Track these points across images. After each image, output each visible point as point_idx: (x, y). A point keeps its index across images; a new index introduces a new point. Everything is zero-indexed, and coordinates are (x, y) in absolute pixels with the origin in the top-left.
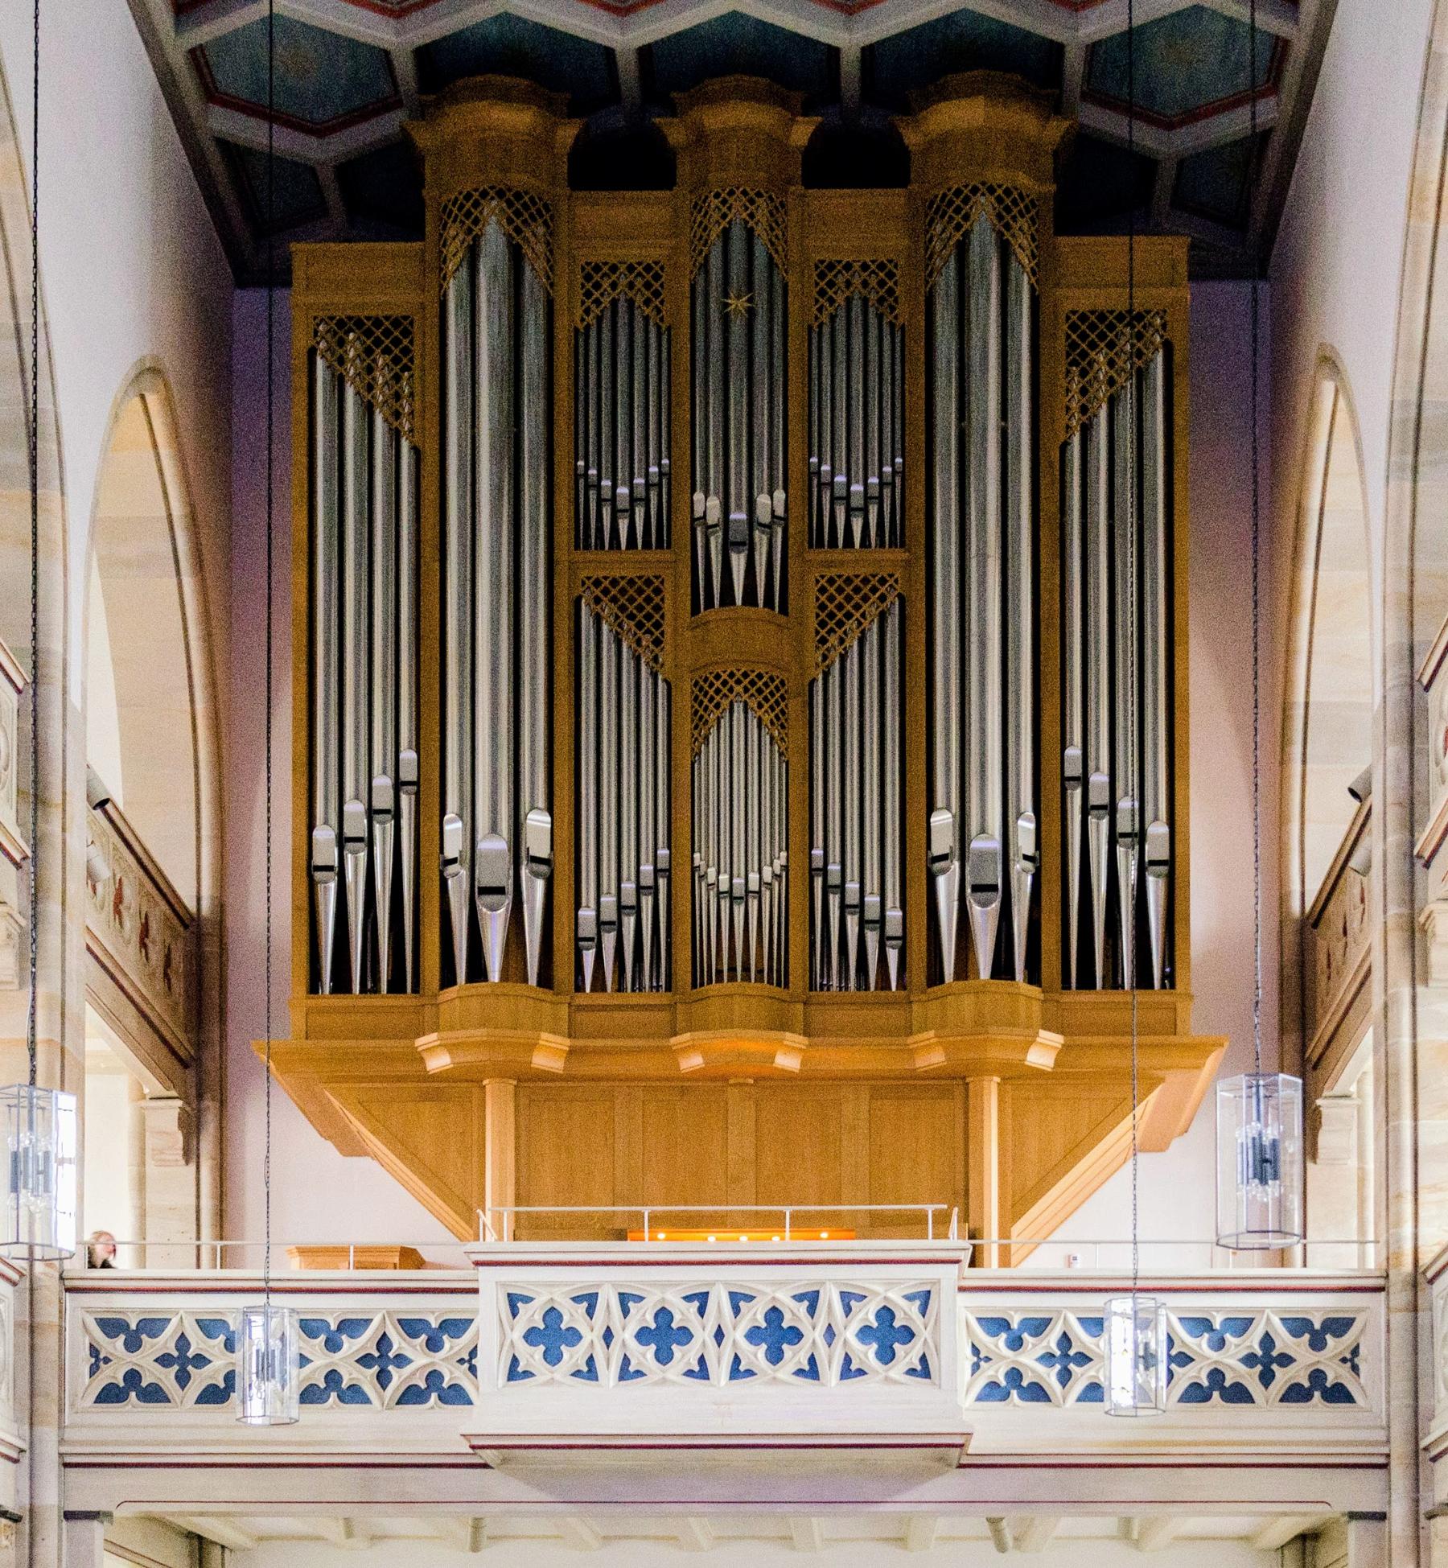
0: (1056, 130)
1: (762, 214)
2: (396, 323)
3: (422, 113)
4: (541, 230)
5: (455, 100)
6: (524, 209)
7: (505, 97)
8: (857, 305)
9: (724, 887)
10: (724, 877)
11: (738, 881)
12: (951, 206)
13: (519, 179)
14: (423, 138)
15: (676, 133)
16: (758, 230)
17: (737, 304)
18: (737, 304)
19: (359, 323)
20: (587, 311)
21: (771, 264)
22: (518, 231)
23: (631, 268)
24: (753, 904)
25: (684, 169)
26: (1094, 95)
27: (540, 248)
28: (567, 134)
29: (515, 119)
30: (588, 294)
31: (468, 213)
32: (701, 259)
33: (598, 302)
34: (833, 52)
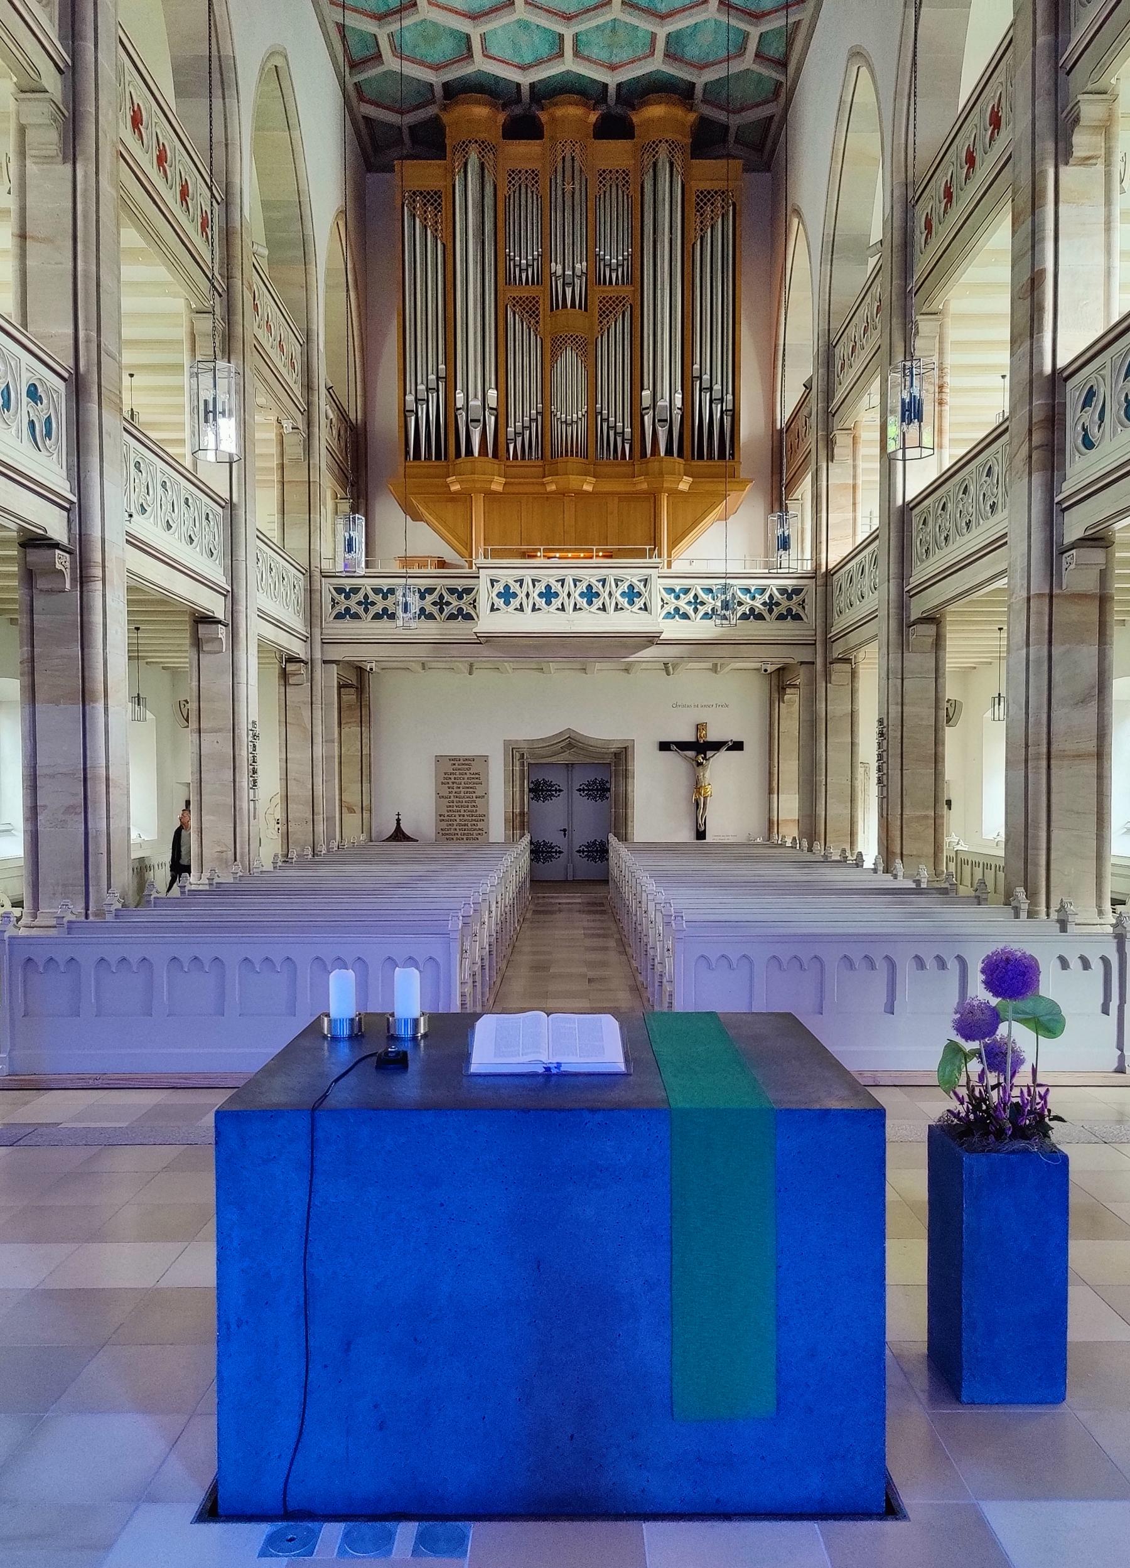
2: (436, 193)
3: (445, 108)
4: (492, 156)
5: (457, 103)
6: (483, 146)
7: (478, 103)
12: (653, 147)
13: (483, 136)
14: (446, 118)
15: (544, 117)
17: (568, 187)
18: (568, 187)
21: (581, 171)
28: (501, 118)
29: (481, 111)
34: (605, 86)
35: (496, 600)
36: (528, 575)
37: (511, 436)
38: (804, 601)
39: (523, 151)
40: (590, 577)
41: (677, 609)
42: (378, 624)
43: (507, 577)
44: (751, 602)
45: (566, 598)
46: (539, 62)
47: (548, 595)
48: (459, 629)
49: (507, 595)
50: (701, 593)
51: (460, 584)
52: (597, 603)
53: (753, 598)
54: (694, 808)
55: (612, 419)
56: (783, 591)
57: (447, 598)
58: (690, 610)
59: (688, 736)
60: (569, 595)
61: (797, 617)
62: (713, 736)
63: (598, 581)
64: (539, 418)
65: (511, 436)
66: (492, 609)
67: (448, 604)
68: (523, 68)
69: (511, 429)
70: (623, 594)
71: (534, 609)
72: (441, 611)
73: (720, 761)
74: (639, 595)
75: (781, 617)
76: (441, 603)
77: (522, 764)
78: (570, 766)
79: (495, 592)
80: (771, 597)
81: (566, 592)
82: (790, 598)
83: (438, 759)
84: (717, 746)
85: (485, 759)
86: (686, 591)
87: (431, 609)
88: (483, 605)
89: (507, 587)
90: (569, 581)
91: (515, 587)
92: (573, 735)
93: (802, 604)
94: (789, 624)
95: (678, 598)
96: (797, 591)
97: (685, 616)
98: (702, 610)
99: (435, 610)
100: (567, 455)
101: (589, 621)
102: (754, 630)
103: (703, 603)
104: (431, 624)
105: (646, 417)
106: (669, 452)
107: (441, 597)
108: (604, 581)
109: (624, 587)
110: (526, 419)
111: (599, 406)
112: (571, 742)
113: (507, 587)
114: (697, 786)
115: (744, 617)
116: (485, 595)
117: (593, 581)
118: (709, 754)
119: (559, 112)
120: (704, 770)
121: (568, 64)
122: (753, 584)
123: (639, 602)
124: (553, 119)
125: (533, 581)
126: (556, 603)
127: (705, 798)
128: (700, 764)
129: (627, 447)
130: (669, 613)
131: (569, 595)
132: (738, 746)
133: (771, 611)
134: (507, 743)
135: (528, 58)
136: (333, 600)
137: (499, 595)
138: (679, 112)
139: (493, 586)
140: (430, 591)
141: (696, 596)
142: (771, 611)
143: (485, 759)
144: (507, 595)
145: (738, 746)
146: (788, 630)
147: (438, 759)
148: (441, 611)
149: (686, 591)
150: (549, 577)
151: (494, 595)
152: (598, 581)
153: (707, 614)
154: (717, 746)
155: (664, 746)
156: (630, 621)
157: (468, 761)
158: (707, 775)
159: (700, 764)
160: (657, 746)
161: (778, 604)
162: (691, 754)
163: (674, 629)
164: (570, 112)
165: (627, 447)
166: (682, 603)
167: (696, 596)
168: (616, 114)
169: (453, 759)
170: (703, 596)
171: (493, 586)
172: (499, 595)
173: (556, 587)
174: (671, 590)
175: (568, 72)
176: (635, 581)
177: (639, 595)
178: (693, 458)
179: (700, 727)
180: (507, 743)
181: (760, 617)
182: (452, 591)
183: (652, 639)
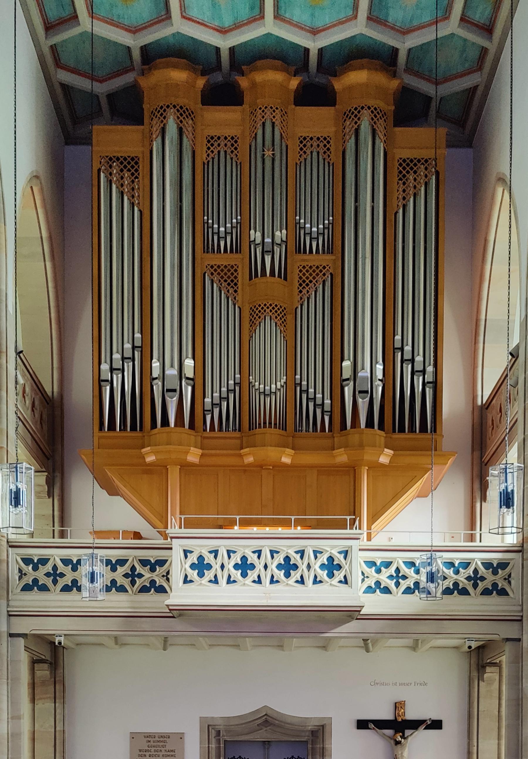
0: (395, 84)
1: (278, 117)
2: (133, 159)
3: (143, 73)
4: (190, 122)
5: (156, 68)
6: (184, 113)
8: (315, 154)
9: (262, 390)
10: (262, 386)
11: (267, 388)
12: (354, 114)
13: (181, 101)
14: (144, 83)
15: (243, 82)
16: (277, 123)
17: (268, 153)
18: (268, 153)
19: (118, 159)
20: (208, 155)
21: (282, 137)
22: (181, 122)
23: (226, 138)
24: (273, 397)
25: (247, 98)
26: (408, 70)
27: (190, 129)
28: (201, 82)
30: (209, 148)
31: (161, 113)
32: (253, 135)
33: (212, 152)
34: (307, 51)
35: (190, 571)
36: (223, 546)
37: (208, 407)
38: (510, 576)
39: (223, 120)
40: (288, 548)
41: (378, 583)
42: (66, 596)
43: (201, 548)
44: (455, 577)
45: (263, 569)
46: (237, 26)
47: (244, 567)
48: (151, 602)
49: (201, 566)
50: (403, 567)
51: (152, 555)
52: (295, 575)
53: (457, 572)
55: (311, 390)
56: (488, 565)
57: (139, 569)
58: (392, 584)
59: (387, 715)
60: (266, 567)
61: (503, 592)
62: (411, 714)
63: (297, 552)
64: (237, 389)
65: (208, 407)
66: (186, 581)
67: (140, 576)
68: (223, 31)
69: (208, 400)
70: (322, 566)
71: (229, 581)
72: (133, 583)
74: (339, 567)
75: (486, 592)
76: (132, 575)
77: (218, 742)
78: (266, 744)
79: (189, 562)
80: (476, 571)
81: (263, 564)
82: (495, 573)
83: (133, 736)
84: (415, 725)
85: (181, 736)
86: (388, 565)
87: (121, 581)
88: (177, 577)
89: (201, 558)
90: (266, 553)
91: (209, 558)
92: (269, 713)
93: (508, 579)
94: (494, 599)
95: (379, 571)
96: (503, 565)
97: (387, 590)
98: (404, 584)
99: (126, 583)
100: (265, 427)
101: (287, 594)
102: (457, 605)
103: (405, 577)
104: (122, 597)
105: (346, 389)
106: (370, 424)
107: (133, 568)
108: (302, 553)
109: (323, 559)
110: (224, 389)
111: (298, 377)
112: (267, 720)
113: (201, 558)
115: (447, 592)
116: (178, 566)
117: (291, 553)
118: (408, 732)
119: (260, 77)
121: (270, 27)
122: (457, 558)
123: (339, 575)
124: (254, 85)
125: (229, 552)
126: (252, 575)
128: (398, 743)
129: (327, 419)
130: (370, 587)
131: (266, 567)
132: (436, 725)
133: (475, 586)
134: (202, 719)
135: (227, 22)
136: (20, 571)
137: (193, 566)
138: (380, 79)
139: (186, 557)
140: (122, 562)
141: (398, 570)
142: (475, 586)
143: (181, 736)
144: (201, 566)
145: (436, 725)
146: (493, 605)
147: (133, 736)
148: (133, 583)
149: (388, 565)
150: (245, 548)
151: (187, 566)
152: (297, 552)
153: (408, 588)
154: (415, 725)
155: (362, 724)
156: (329, 594)
157: (164, 737)
158: (405, 754)
159: (398, 743)
160: (355, 724)
161: (483, 579)
162: (389, 732)
163: (375, 604)
164: (271, 77)
165: (327, 419)
166: (384, 577)
167: (398, 570)
168: (315, 81)
169: (148, 736)
170: (405, 570)
171: (186, 557)
172: (193, 566)
173: (252, 558)
174: (371, 564)
175: (269, 35)
176: (335, 552)
177: (339, 567)
178: (394, 431)
180: (202, 719)
181: (464, 592)
182: (144, 563)
183: (352, 614)
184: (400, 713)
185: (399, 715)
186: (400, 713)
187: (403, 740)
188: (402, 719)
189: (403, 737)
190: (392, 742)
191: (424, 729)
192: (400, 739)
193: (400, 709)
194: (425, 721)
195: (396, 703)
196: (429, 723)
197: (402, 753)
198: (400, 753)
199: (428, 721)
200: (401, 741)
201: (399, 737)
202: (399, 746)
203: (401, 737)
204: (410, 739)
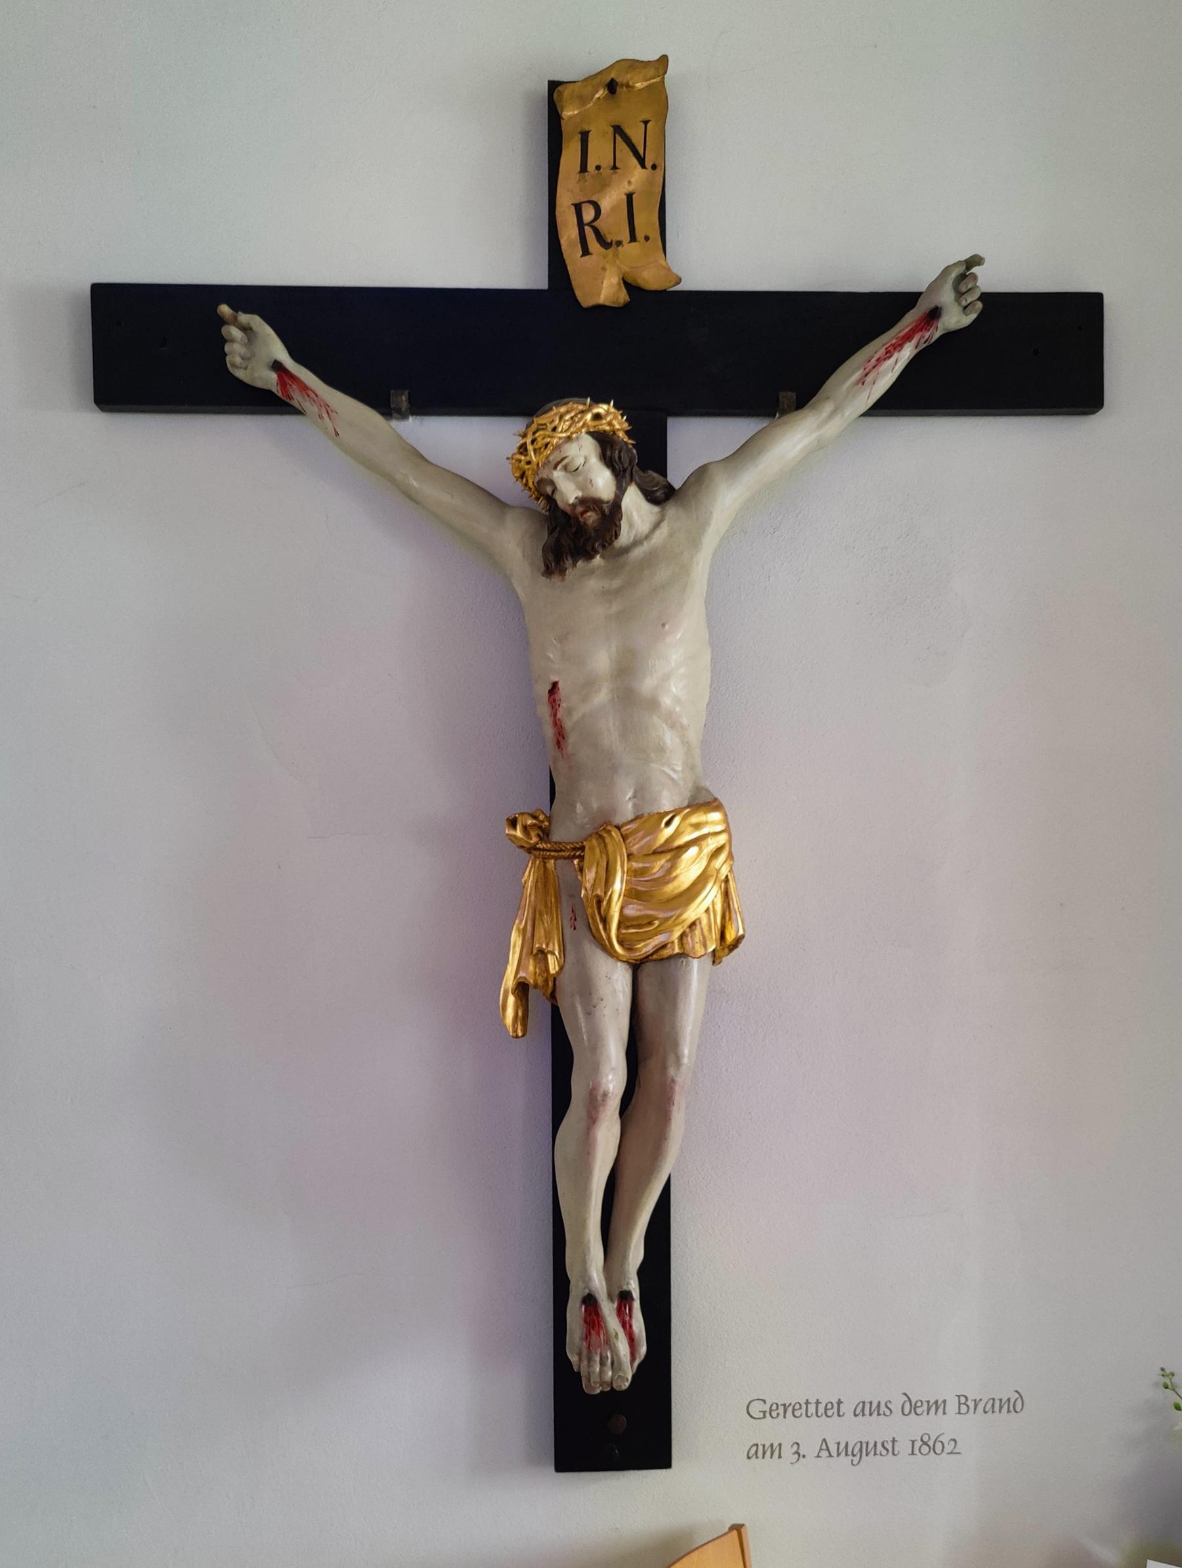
54: (525, 1077)
62: (735, 230)
73: (814, 508)
84: (775, 351)
114: (558, 830)
118: (692, 441)
120: (643, 593)
127: (654, 975)
128: (573, 537)
132: (1027, 355)
145: (1027, 355)
154: (775, 351)
158: (678, 671)
159: (573, 537)
160: (69, 349)
179: (595, 128)
184: (611, 200)
185: (594, 235)
186: (611, 200)
187: (636, 508)
188: (631, 287)
189: (641, 458)
190: (515, 543)
191: (892, 404)
192: (603, 482)
193: (600, 151)
194: (903, 301)
195: (553, 85)
196: (955, 319)
197: (627, 669)
198: (602, 660)
199: (946, 297)
200: (611, 514)
201: (584, 451)
202: (590, 578)
203: (604, 440)
204: (727, 500)
